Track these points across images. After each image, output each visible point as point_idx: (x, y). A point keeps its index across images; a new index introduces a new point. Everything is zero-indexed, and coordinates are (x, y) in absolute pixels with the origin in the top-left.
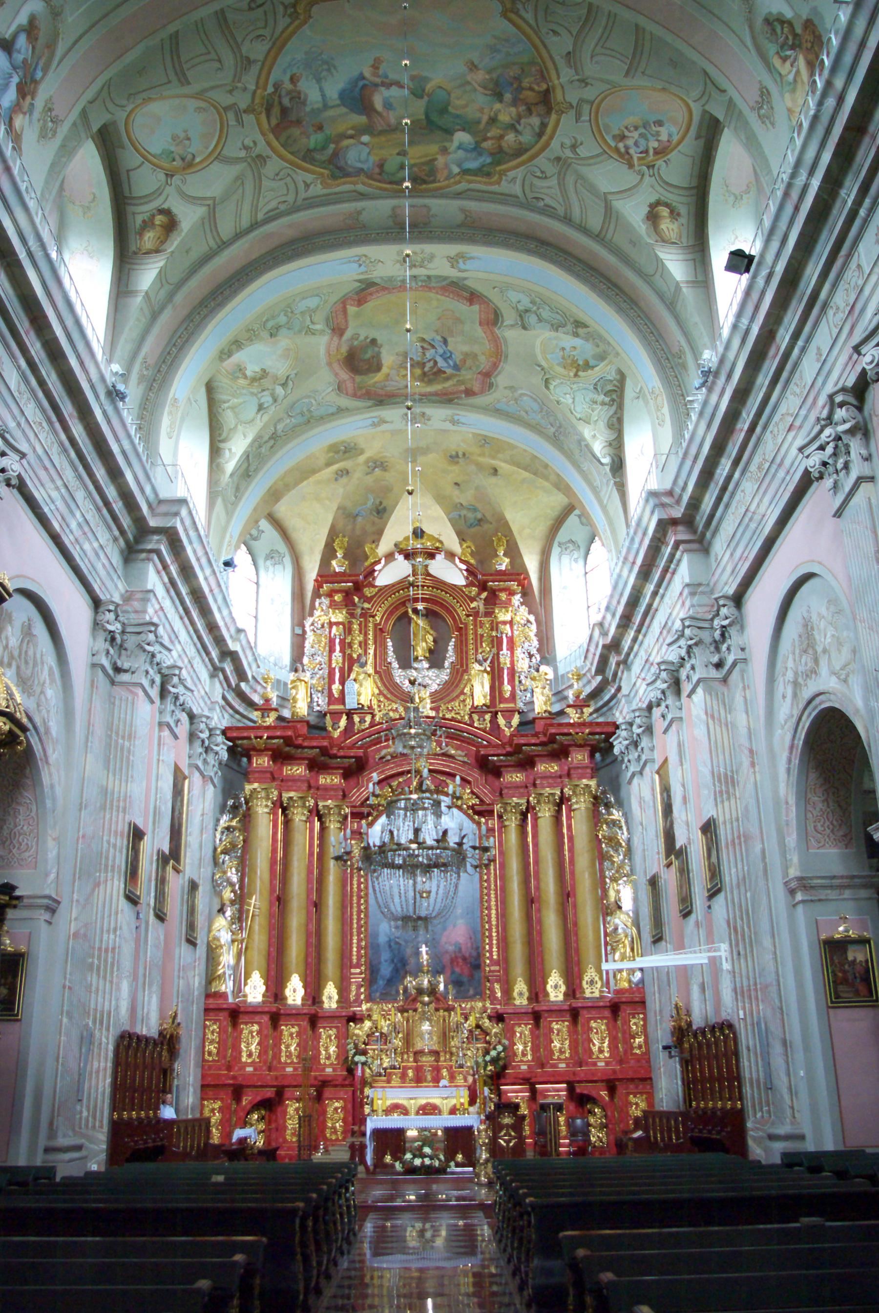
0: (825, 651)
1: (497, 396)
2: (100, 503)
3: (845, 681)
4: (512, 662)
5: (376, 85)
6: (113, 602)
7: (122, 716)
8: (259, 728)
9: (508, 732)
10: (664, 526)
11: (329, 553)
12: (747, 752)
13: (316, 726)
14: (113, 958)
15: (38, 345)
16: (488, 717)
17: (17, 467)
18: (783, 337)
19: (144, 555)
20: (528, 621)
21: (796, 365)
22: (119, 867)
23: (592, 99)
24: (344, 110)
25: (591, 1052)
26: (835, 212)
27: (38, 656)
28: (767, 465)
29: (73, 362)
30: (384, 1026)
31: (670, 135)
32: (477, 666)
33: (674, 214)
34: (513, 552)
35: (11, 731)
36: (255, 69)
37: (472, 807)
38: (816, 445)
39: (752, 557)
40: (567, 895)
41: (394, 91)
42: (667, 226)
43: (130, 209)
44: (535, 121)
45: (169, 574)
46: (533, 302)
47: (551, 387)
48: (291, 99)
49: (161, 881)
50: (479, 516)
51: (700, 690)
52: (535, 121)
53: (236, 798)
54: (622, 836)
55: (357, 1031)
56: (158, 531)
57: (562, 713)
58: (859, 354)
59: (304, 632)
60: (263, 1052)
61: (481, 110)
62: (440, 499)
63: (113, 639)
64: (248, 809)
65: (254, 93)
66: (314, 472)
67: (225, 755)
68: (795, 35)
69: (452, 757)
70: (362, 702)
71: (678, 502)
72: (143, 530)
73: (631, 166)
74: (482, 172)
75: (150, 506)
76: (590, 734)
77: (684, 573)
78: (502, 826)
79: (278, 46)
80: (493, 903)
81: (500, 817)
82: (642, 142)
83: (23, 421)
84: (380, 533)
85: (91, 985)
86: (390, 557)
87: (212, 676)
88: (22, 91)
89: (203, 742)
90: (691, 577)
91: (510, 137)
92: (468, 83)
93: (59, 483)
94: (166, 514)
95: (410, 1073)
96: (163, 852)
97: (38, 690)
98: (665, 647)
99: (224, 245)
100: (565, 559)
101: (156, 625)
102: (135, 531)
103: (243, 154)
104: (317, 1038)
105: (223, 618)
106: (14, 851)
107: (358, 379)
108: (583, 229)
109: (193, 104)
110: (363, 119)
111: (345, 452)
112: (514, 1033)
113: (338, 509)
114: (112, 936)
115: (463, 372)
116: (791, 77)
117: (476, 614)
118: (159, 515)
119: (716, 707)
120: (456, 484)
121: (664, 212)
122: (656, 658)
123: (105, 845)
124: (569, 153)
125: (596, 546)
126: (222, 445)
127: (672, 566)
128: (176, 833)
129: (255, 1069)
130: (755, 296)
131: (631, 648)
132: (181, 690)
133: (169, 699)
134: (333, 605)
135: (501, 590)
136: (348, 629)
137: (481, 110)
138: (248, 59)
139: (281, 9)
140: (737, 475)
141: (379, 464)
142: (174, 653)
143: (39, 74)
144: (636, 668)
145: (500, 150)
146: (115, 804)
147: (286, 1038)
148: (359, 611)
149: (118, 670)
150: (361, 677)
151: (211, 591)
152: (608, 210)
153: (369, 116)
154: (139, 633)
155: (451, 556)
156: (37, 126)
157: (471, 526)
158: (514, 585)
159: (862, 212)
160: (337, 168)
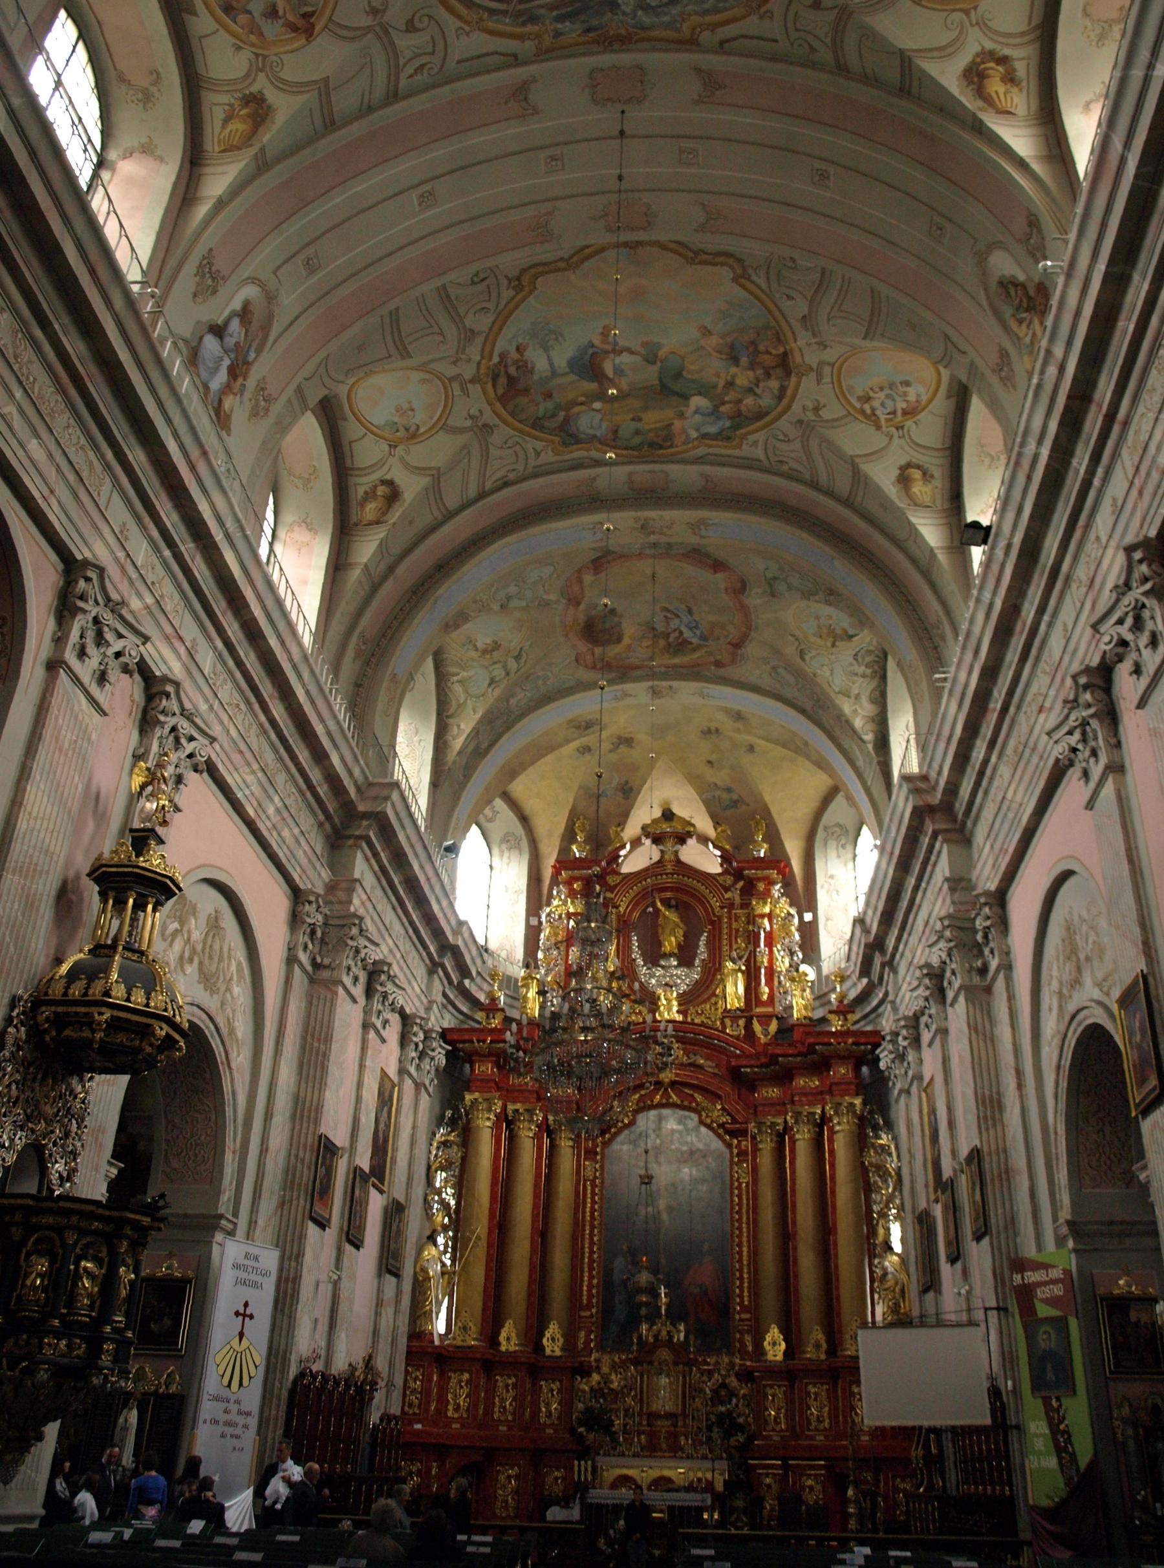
0: (1088, 959)
1: (750, 671)
2: (304, 787)
3: (1108, 994)
5: (607, 352)
8: (481, 1030)
10: (920, 814)
11: (569, 836)
12: (1013, 1072)
13: (548, 1029)
15: (236, 626)
16: (742, 1022)
18: (1029, 612)
19: (351, 842)
20: (789, 914)
21: (1044, 642)
23: (832, 360)
24: (573, 377)
26: (1068, 482)
27: (225, 950)
29: (273, 642)
31: (918, 396)
32: (730, 965)
33: (927, 476)
34: (774, 838)
36: (479, 340)
37: (722, 1126)
38: (1065, 729)
39: (1011, 850)
41: (625, 358)
42: (919, 489)
43: (353, 480)
44: (774, 384)
46: (781, 569)
47: (807, 658)
48: (518, 368)
50: (735, 797)
51: (961, 999)
52: (774, 384)
53: (456, 1109)
54: (892, 1165)
56: (366, 815)
57: (823, 1020)
59: (540, 923)
61: (718, 375)
62: (694, 779)
64: (468, 1121)
65: (479, 363)
66: (551, 748)
68: (1029, 298)
69: (700, 1067)
71: (934, 788)
73: (878, 427)
74: (721, 437)
75: (359, 789)
76: (854, 1043)
77: (943, 868)
78: (756, 1150)
79: (503, 317)
80: (744, 1239)
81: (754, 1138)
82: (889, 403)
83: (216, 704)
86: (636, 843)
87: (431, 972)
88: (233, 372)
89: (417, 1045)
90: (951, 870)
91: (749, 401)
92: (702, 348)
93: (255, 766)
94: (375, 798)
99: (450, 515)
101: (361, 919)
103: (468, 423)
104: (536, 1391)
105: (442, 909)
106: (190, 1164)
107: (598, 651)
108: (830, 493)
109: (416, 376)
110: (594, 386)
111: (587, 728)
112: (766, 1396)
113: (580, 787)
114: (293, 1264)
116: (1028, 340)
119: (979, 1020)
120: (710, 762)
121: (916, 474)
122: (920, 959)
124: (810, 416)
125: (865, 831)
126: (450, 721)
127: (933, 858)
128: (380, 1148)
129: (463, 1426)
130: (995, 568)
131: (896, 948)
132: (390, 987)
134: (572, 894)
135: (759, 879)
137: (718, 375)
138: (472, 331)
139: (505, 282)
140: (994, 759)
141: (626, 741)
142: (384, 947)
143: (252, 355)
144: (902, 970)
145: (739, 414)
147: (500, 1390)
151: (428, 879)
152: (856, 472)
153: (600, 383)
156: (248, 406)
157: (725, 808)
159: (1096, 482)
160: (568, 435)
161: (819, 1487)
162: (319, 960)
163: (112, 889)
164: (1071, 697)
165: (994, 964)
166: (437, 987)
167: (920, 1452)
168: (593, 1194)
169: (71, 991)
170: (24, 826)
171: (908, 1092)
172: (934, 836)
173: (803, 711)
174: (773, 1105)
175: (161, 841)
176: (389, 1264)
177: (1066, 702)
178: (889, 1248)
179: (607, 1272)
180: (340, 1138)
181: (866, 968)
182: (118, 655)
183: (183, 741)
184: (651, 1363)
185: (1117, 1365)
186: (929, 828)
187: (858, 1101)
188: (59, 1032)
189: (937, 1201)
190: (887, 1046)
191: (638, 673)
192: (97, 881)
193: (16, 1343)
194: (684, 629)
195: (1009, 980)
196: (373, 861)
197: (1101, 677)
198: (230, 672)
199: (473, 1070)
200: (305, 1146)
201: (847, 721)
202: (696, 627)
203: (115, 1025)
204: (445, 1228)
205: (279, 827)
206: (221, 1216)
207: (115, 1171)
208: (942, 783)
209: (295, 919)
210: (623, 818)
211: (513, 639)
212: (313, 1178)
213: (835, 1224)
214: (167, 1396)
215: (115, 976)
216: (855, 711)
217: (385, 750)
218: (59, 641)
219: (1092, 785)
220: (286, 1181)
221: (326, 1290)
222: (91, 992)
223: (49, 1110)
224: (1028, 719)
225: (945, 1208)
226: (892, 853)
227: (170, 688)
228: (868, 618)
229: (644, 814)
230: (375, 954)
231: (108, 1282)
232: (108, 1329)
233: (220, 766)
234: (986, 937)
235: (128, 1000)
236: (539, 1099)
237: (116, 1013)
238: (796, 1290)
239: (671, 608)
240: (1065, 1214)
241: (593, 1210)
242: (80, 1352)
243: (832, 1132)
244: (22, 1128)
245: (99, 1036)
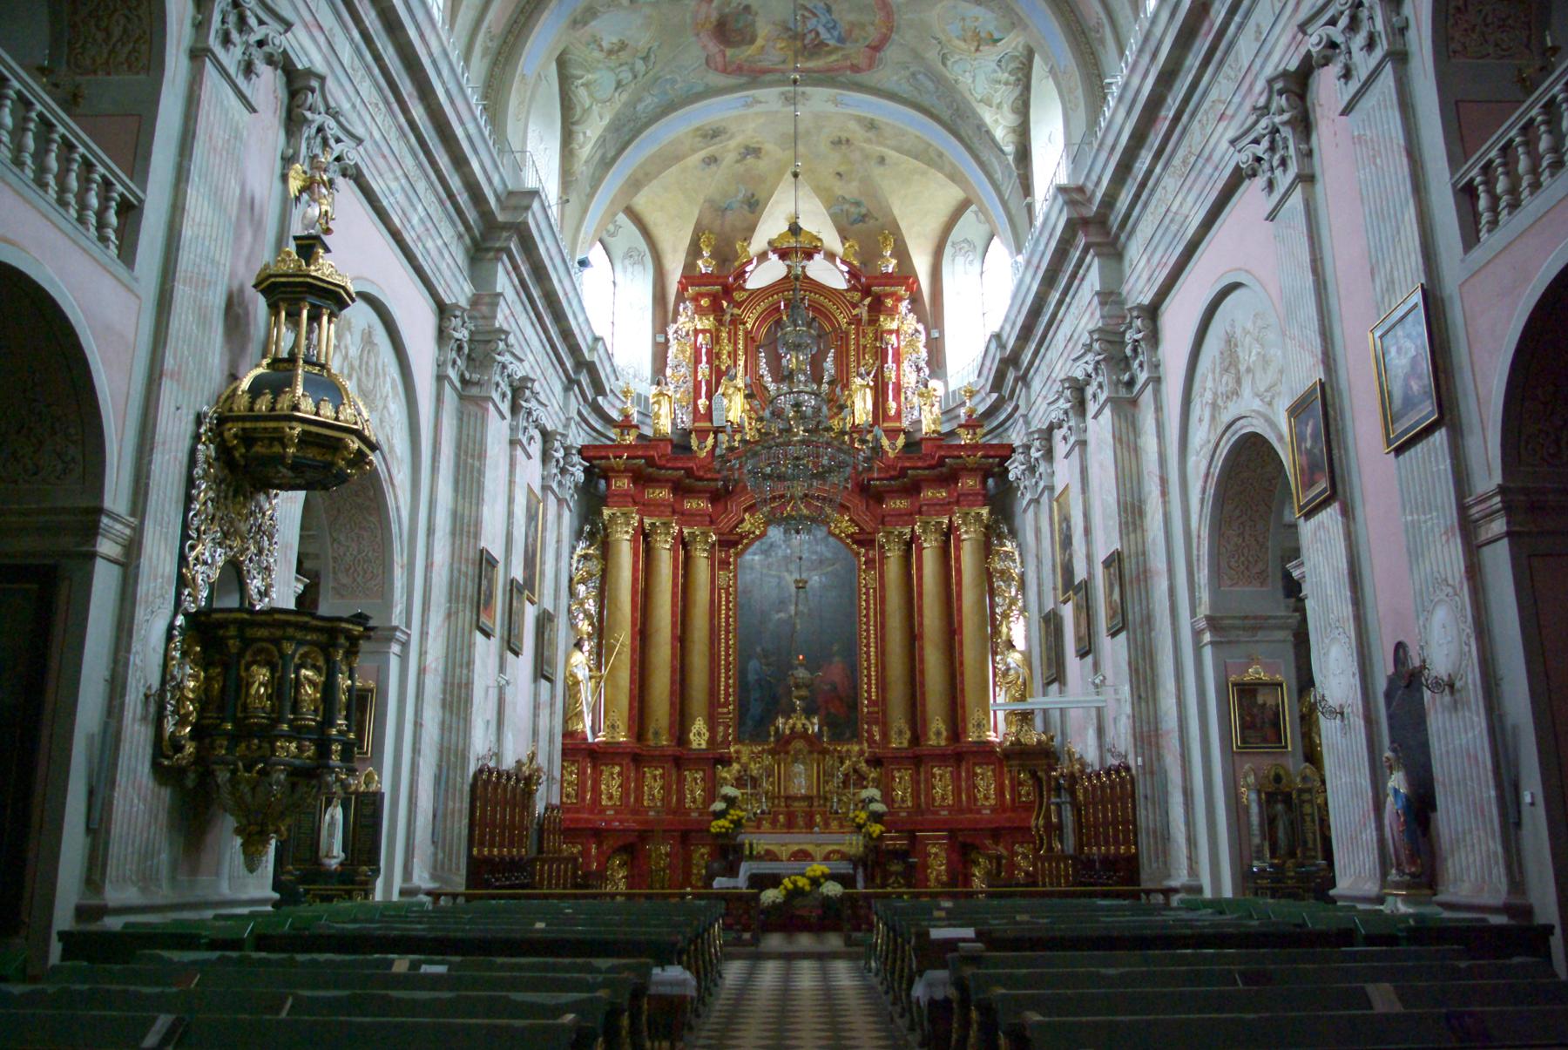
0: (1248, 370)
1: (886, 76)
2: (444, 196)
3: (1270, 404)
4: (898, 376)
9: (891, 454)
10: (1072, 227)
11: (694, 251)
13: (680, 444)
15: (373, 14)
19: (491, 254)
25: (976, 799)
28: (1192, 159)
30: (754, 769)
32: (858, 381)
34: (902, 254)
35: (359, 449)
38: (1251, 137)
40: (952, 631)
47: (949, 63)
50: (864, 211)
54: (1016, 571)
55: (725, 775)
57: (952, 433)
58: (1305, 33)
59: (667, 341)
60: (625, 794)
62: (821, 192)
64: (607, 536)
66: (678, 158)
67: (581, 477)
70: (731, 418)
71: (1090, 200)
77: (1093, 280)
78: (883, 558)
84: (751, 229)
86: (763, 257)
87: (567, 389)
93: (399, 173)
94: (516, 208)
95: (781, 818)
97: (380, 404)
98: (1070, 362)
100: (960, 260)
101: (507, 333)
104: (681, 781)
106: (359, 579)
107: (729, 52)
112: (893, 778)
115: (848, 45)
117: (857, 320)
122: (1060, 373)
126: (576, 128)
127: (1081, 272)
128: (530, 562)
129: (617, 812)
131: (1031, 363)
132: (533, 404)
133: (522, 414)
134: (700, 311)
136: (716, 339)
140: (1158, 170)
141: (753, 151)
142: (526, 364)
144: (1036, 384)
148: (728, 318)
150: (731, 391)
155: (831, 256)
157: (855, 222)
158: (902, 291)
161: (943, 854)
162: (467, 376)
163: (283, 300)
164: (1262, 101)
165: (1142, 377)
166: (574, 405)
167: (1041, 822)
168: (728, 602)
169: (257, 407)
171: (1037, 501)
172: (1086, 251)
173: (937, 119)
174: (900, 515)
175: (327, 250)
176: (542, 671)
177: (1255, 108)
178: (1010, 645)
179: (742, 674)
180: (497, 552)
181: (997, 384)
182: (260, 44)
183: (332, 142)
184: (787, 753)
185: (1244, 740)
186: (1081, 241)
187: (985, 511)
189: (1065, 602)
190: (1018, 457)
191: (768, 77)
192: (263, 292)
194: (821, 30)
195: (1157, 393)
196: (513, 275)
197: (1298, 83)
198: (368, 67)
199: (608, 485)
201: (988, 132)
202: (834, 27)
203: (306, 440)
204: (589, 635)
206: (396, 628)
207: (301, 587)
208: (1099, 195)
209: (442, 335)
210: (749, 232)
211: (642, 39)
212: (479, 589)
213: (960, 623)
214: (365, 794)
215: (300, 391)
216: (996, 121)
217: (518, 156)
218: (200, 26)
219: (1276, 196)
220: (450, 594)
221: (493, 693)
222: (278, 406)
223: (244, 527)
224: (1203, 128)
225: (1077, 608)
226: (1038, 267)
227: (315, 84)
228: (1020, 19)
229: (771, 227)
230: (520, 370)
231: (329, 689)
232: (334, 731)
233: (365, 171)
234: (1135, 350)
235: (317, 414)
236: (674, 512)
237: (307, 427)
238: (922, 685)
239: (810, 6)
240: (1204, 610)
241: (727, 617)
242: (309, 753)
243: (959, 540)
244: (220, 545)
245: (291, 450)
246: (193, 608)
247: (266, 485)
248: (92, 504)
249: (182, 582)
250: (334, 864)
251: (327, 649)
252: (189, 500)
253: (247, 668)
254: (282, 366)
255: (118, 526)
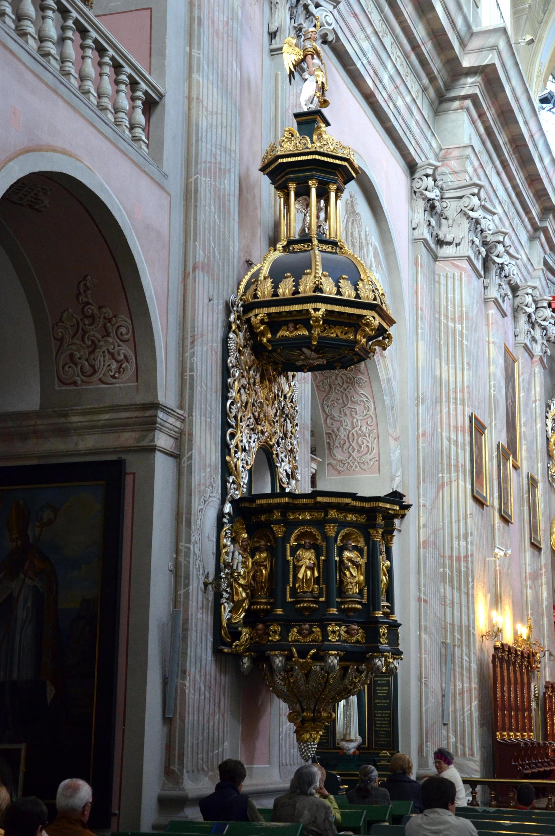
2: (408, 48)
6: (430, 165)
7: (450, 295)
14: (467, 568)
17: (330, 19)
19: (456, 104)
22: (464, 466)
27: (363, 236)
45: (485, 123)
49: (503, 482)
56: (472, 71)
63: (433, 207)
72: (456, 72)
85: (445, 597)
87: (532, 239)
89: (529, 316)
93: (369, 30)
96: (503, 446)
101: (480, 187)
102: (446, 76)
105: (545, 168)
114: (463, 543)
118: (473, 51)
123: (445, 442)
132: (505, 259)
133: (494, 270)
146: (452, 395)
149: (440, 243)
151: (532, 136)
154: (461, 197)
163: (292, 180)
169: (280, 291)
170: (205, 124)
175: (328, 124)
188: (274, 333)
192: (270, 175)
193: (299, 632)
200: (456, 427)
205: (394, 96)
244: (252, 429)
245: (316, 332)
246: (238, 495)
247: (290, 366)
248: (149, 400)
249: (227, 470)
250: (351, 747)
251: (365, 529)
252: (226, 388)
253: (294, 551)
254: (296, 247)
255: (171, 420)
